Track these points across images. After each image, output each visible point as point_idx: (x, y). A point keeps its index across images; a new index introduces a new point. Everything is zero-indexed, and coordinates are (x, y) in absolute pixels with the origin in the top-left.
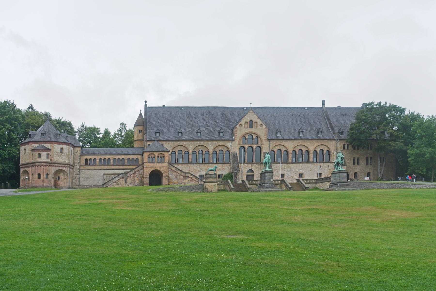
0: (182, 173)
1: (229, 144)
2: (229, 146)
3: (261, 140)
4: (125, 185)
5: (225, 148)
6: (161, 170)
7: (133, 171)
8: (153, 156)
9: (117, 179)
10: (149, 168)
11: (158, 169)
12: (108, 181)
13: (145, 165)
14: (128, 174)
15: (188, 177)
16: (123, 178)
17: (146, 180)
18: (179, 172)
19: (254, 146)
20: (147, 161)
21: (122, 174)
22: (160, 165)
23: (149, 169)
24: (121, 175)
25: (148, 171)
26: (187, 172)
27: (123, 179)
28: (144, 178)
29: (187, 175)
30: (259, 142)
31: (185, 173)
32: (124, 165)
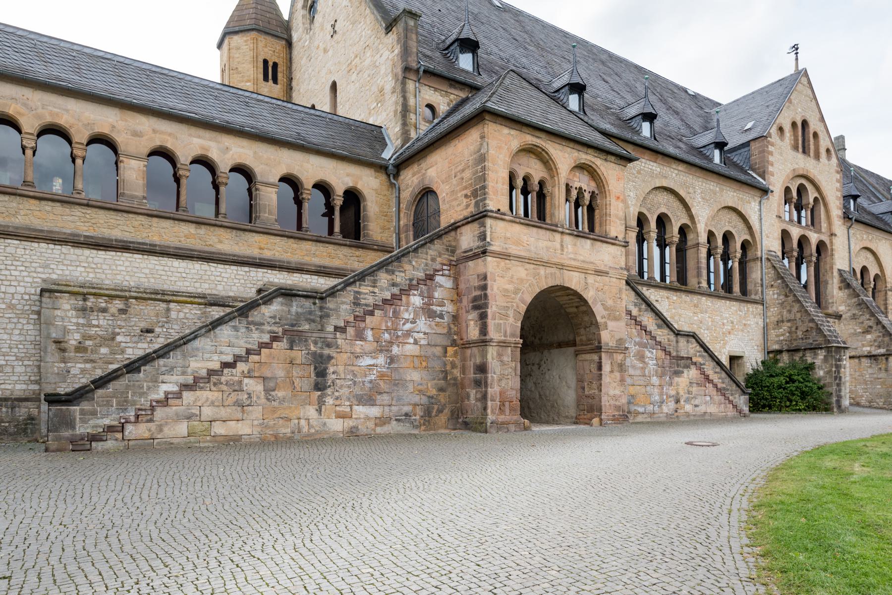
0: (663, 335)
1: (751, 206)
2: (754, 220)
3: (828, 217)
4: (311, 412)
5: (741, 225)
6: (589, 295)
7: (383, 278)
8: (537, 172)
9: (231, 340)
10: (520, 263)
11: (573, 281)
12: (133, 367)
13: (504, 234)
14: (342, 308)
15: (688, 362)
16: (294, 337)
17: (504, 373)
18: (648, 320)
19: (814, 238)
20: (505, 208)
21: (288, 293)
22: (584, 251)
23: (520, 271)
24: (276, 307)
25: (511, 288)
26: (686, 328)
27: (299, 355)
28: (492, 352)
29: (688, 348)
30: (824, 225)
31: (678, 334)
32: (250, 219)
